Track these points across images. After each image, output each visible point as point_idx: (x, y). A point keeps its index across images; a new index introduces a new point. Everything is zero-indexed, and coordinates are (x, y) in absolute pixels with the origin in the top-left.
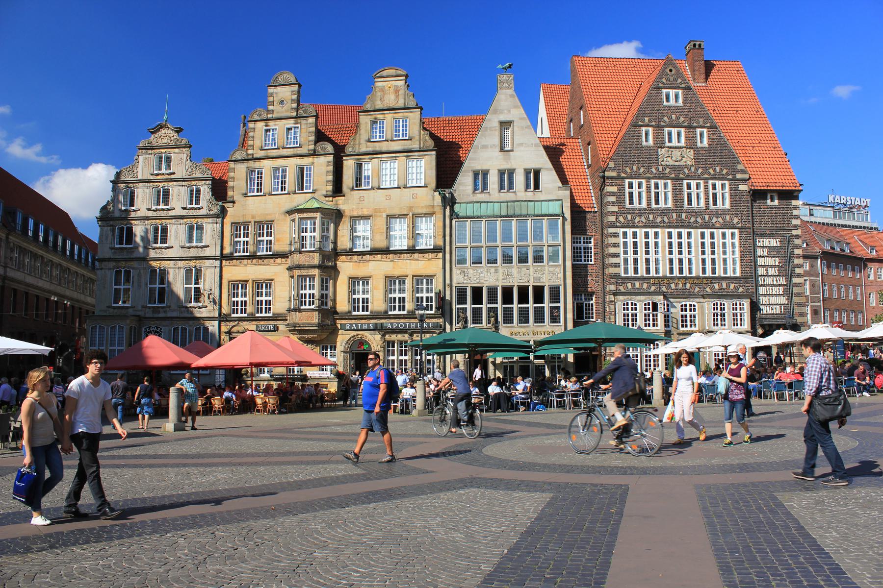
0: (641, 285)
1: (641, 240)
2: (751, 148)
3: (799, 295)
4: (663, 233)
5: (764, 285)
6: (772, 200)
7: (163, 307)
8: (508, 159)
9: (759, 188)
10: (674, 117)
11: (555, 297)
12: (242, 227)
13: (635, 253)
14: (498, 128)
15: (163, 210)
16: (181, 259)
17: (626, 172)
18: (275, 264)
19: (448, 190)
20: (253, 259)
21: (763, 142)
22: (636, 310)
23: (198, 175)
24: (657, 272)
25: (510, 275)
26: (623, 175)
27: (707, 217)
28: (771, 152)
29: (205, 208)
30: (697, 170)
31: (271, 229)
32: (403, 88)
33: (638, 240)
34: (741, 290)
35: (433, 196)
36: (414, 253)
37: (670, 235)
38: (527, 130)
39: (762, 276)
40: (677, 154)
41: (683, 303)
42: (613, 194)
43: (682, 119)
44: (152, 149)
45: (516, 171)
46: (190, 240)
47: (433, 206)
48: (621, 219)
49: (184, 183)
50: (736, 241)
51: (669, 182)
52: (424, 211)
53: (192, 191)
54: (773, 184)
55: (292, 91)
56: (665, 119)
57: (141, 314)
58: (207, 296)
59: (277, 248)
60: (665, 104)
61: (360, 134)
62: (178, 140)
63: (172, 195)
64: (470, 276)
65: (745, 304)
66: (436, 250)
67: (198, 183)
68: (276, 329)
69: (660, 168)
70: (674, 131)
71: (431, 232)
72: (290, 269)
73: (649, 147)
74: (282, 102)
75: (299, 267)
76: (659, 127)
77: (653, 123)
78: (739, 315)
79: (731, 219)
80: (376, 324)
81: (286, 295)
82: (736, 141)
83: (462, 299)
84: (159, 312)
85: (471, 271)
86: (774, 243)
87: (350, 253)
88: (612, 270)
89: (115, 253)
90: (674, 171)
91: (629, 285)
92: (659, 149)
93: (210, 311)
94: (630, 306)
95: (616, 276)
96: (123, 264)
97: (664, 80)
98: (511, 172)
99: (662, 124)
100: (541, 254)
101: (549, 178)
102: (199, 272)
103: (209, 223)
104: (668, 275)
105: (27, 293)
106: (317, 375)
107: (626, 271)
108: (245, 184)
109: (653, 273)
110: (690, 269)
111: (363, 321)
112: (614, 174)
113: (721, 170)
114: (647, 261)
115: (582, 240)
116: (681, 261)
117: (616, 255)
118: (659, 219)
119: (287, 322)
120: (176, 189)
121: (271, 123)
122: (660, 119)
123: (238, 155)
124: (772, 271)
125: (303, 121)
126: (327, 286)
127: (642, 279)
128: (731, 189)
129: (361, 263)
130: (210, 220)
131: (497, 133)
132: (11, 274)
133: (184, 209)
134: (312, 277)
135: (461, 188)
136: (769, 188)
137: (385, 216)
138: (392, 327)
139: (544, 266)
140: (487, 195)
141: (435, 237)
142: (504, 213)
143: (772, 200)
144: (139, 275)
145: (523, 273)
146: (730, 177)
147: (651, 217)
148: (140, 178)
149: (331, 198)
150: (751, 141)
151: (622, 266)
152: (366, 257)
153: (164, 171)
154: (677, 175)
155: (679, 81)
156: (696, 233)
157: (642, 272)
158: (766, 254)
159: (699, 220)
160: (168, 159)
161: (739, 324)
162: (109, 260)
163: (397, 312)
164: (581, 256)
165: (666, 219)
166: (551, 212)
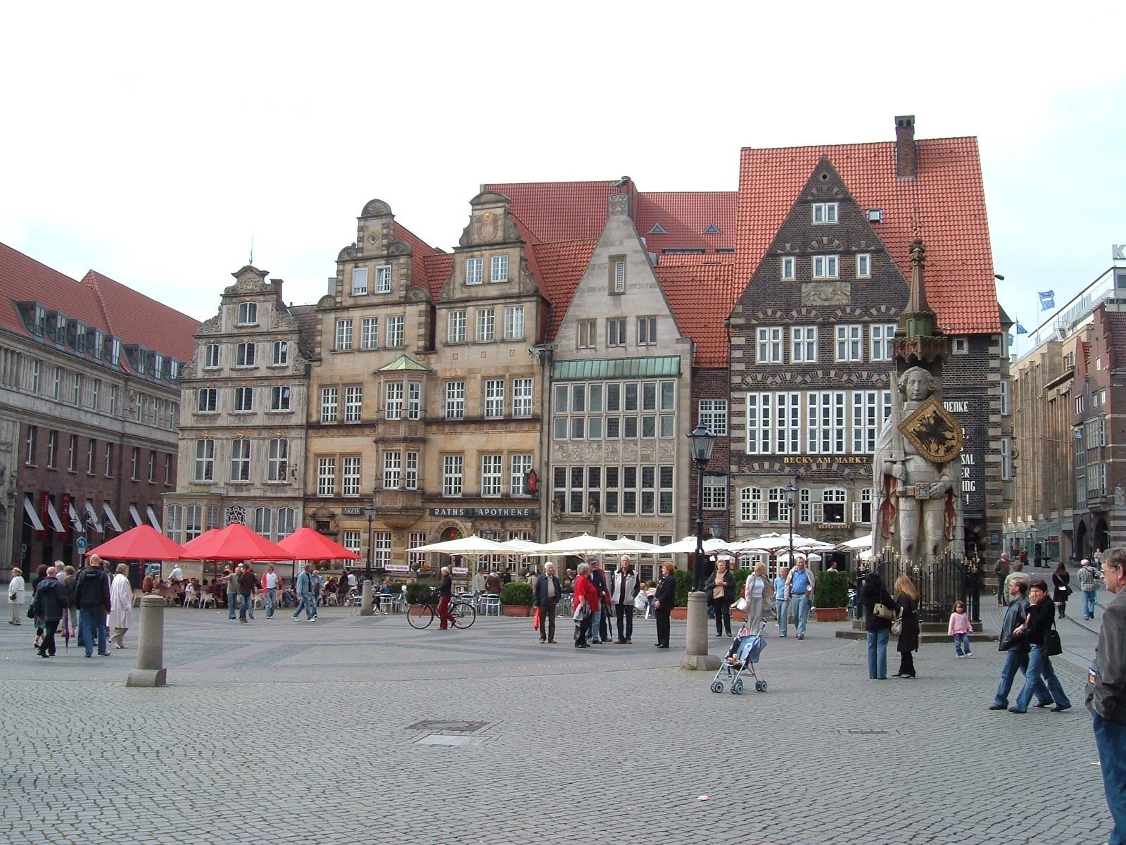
0: (772, 466)
1: (774, 406)
3: (994, 478)
4: (804, 397)
7: (247, 485)
8: (617, 305)
10: (825, 239)
11: (666, 480)
13: (766, 423)
15: (246, 369)
17: (757, 318)
18: (363, 436)
19: (549, 345)
23: (284, 328)
24: (795, 447)
25: (615, 452)
26: (754, 322)
27: (865, 374)
29: (291, 367)
30: (853, 311)
33: (770, 407)
41: (828, 489)
42: (738, 347)
43: (837, 242)
44: (236, 297)
45: (628, 319)
46: (275, 406)
49: (269, 338)
52: (522, 371)
55: (383, 224)
56: (814, 243)
57: (221, 491)
60: (814, 223)
63: (257, 352)
66: (536, 420)
67: (284, 337)
68: (362, 514)
69: (804, 311)
70: (825, 259)
72: (376, 442)
73: (790, 283)
76: (804, 257)
77: (797, 251)
80: (467, 510)
81: (372, 472)
83: (560, 480)
84: (242, 491)
87: (440, 422)
88: (734, 446)
91: (756, 466)
92: (804, 285)
95: (741, 456)
96: (205, 434)
97: (814, 191)
98: (623, 322)
99: (809, 250)
101: (667, 329)
102: (284, 443)
103: (295, 385)
104: (809, 452)
107: (753, 448)
112: (741, 321)
113: (888, 309)
115: (713, 405)
118: (799, 379)
120: (261, 345)
122: (806, 244)
125: (395, 262)
126: (414, 463)
127: (773, 458)
129: (453, 436)
130: (296, 382)
131: (607, 271)
132: (130, 429)
133: (268, 368)
135: (564, 342)
137: (479, 377)
138: (484, 512)
139: (655, 440)
140: (593, 351)
142: (610, 373)
147: (788, 376)
148: (223, 331)
149: (423, 356)
151: (748, 440)
152: (459, 428)
155: (836, 190)
156: (848, 396)
157: (774, 449)
159: (854, 378)
160: (253, 307)
162: (192, 429)
165: (808, 379)
166: (666, 371)
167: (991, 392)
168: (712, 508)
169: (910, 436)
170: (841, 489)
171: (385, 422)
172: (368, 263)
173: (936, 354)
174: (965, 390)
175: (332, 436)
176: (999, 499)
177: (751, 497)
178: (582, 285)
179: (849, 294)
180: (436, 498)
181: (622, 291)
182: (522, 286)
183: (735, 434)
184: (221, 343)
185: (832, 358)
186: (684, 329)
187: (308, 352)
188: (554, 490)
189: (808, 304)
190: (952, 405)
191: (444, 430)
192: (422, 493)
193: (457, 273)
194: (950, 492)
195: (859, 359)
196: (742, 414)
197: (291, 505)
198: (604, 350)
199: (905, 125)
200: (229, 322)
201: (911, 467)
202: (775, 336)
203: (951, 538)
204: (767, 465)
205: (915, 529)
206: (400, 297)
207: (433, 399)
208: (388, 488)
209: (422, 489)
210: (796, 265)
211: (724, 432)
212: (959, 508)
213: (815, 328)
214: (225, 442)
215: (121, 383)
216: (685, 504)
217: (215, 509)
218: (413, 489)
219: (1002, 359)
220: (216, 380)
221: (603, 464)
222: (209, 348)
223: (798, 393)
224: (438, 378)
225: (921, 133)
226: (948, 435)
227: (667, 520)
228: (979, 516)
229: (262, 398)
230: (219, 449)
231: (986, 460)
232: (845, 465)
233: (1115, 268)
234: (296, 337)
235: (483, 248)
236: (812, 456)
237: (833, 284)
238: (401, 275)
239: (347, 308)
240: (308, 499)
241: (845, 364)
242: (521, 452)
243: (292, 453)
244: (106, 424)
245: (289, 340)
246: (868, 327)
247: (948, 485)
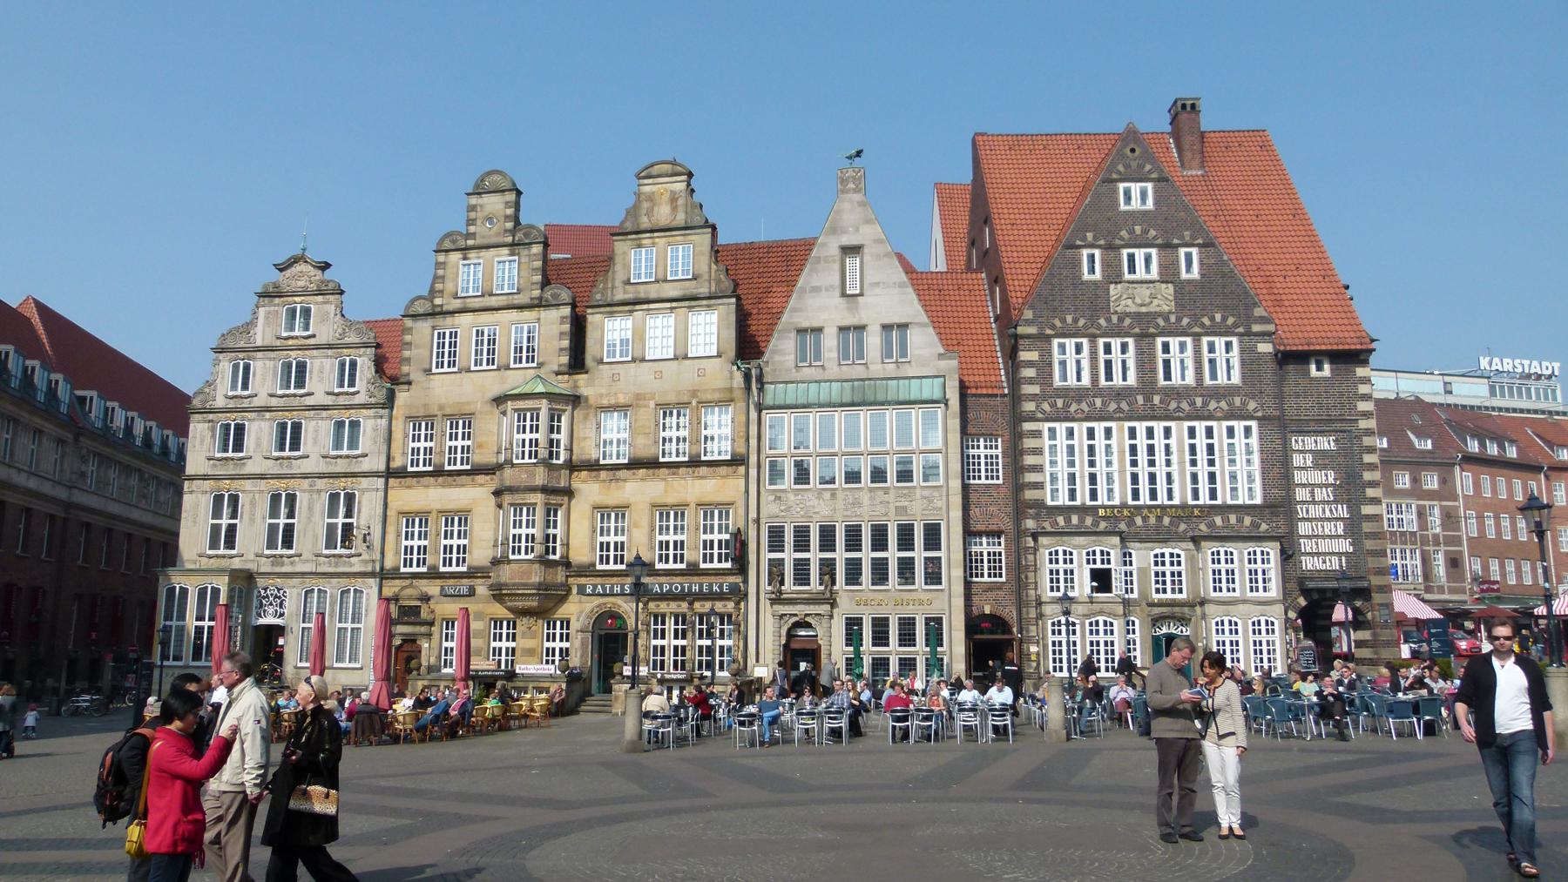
0: (1082, 520)
1: (1081, 441)
2: (1281, 279)
4: (1121, 429)
5: (1308, 520)
6: (1319, 369)
7: (290, 557)
8: (853, 309)
9: (1294, 348)
10: (1138, 229)
12: (423, 424)
14: (838, 258)
16: (321, 476)
17: (1053, 327)
18: (474, 485)
19: (754, 363)
20: (439, 476)
21: (1304, 267)
22: (1071, 561)
23: (352, 338)
25: (857, 503)
26: (1049, 332)
27: (1199, 401)
28: (1318, 285)
29: (363, 392)
30: (1179, 319)
31: (469, 428)
32: (683, 194)
33: (1075, 442)
34: (1264, 527)
35: (731, 372)
36: (699, 466)
37: (1133, 433)
38: (886, 259)
39: (1303, 502)
40: (1143, 293)
41: (1158, 551)
42: (1030, 364)
43: (1153, 233)
45: (868, 328)
46: (338, 444)
47: (731, 390)
48: (1046, 406)
49: (330, 352)
50: (1254, 440)
51: (1130, 341)
52: (716, 396)
53: (342, 365)
54: (1320, 340)
55: (507, 203)
56: (1123, 233)
57: (252, 567)
58: (360, 537)
59: (478, 458)
60: (1123, 207)
61: (614, 272)
62: (322, 282)
63: (311, 372)
64: (790, 504)
65: (1272, 553)
66: (738, 461)
69: (1115, 319)
70: (1139, 254)
71: (727, 431)
72: (497, 493)
73: (1095, 283)
74: (489, 219)
75: (511, 490)
76: (1111, 248)
77: (1102, 242)
78: (1260, 572)
79: (1244, 404)
81: (490, 535)
82: (1254, 268)
85: (791, 497)
86: (1326, 443)
87: (593, 466)
88: (1029, 495)
89: (214, 465)
90: (1139, 323)
91: (1061, 520)
92: (1112, 286)
93: (365, 562)
94: (1061, 557)
95: (1040, 504)
97: (1121, 168)
99: (1118, 242)
100: (907, 467)
101: (923, 342)
102: (350, 498)
103: (369, 417)
104: (1130, 502)
105: (110, 531)
106: (532, 671)
108: (428, 353)
109: (1102, 499)
110: (1170, 491)
111: (615, 580)
112: (1032, 330)
113: (1224, 319)
114: (1093, 478)
116: (1152, 478)
117: (1038, 469)
118: (1113, 406)
119: (490, 581)
120: (317, 362)
121: (472, 254)
122: (1116, 235)
123: (420, 308)
124: (1320, 494)
125: (524, 252)
126: (555, 522)
127: (1083, 510)
128: (1242, 351)
130: (371, 412)
131: (837, 266)
133: (328, 393)
134: (532, 507)
135: (777, 358)
136: (1312, 348)
137: (652, 404)
138: (661, 589)
139: (914, 487)
140: (820, 370)
141: (733, 440)
142: (847, 399)
143: (1319, 369)
144: (253, 503)
145: (878, 501)
146: (1241, 330)
147: (1098, 402)
148: (259, 343)
150: (1281, 267)
152: (622, 473)
153: (296, 333)
154: (1145, 329)
155: (1148, 167)
156: (1179, 428)
157: (1083, 497)
158: (1309, 463)
159: (1185, 405)
160: (306, 312)
161: (1261, 589)
162: (205, 478)
163: (671, 566)
164: (979, 471)
165: (1124, 406)
166: (926, 395)
168: (986, 579)
170: (1176, 551)
171: (513, 465)
172: (484, 253)
174: (1330, 421)
175: (427, 486)
177: (1061, 561)
178: (800, 284)
179: (1171, 298)
180: (588, 570)
181: (858, 292)
182: (713, 284)
183: (1031, 477)
184: (254, 359)
185: (1154, 381)
186: (951, 340)
187: (389, 375)
188: (767, 556)
189: (1118, 309)
190: (1316, 442)
191: (599, 476)
192: (566, 563)
193: (618, 267)
195: (1190, 379)
196: (1038, 452)
197: (359, 583)
198: (836, 368)
199: (1183, 112)
200: (268, 330)
202: (1079, 349)
204: (1075, 519)
206: (531, 299)
207: (582, 435)
208: (516, 557)
209: (567, 557)
210: (1103, 260)
211: (998, 478)
213: (1130, 341)
214: (257, 496)
215: (69, 437)
216: (958, 573)
217: (241, 591)
218: (557, 557)
220: (244, 410)
221: (840, 520)
222: (236, 367)
223: (1113, 424)
224: (589, 407)
225: (1207, 122)
227: (934, 594)
229: (317, 434)
230: (247, 507)
231: (1363, 513)
232: (1179, 517)
234: (371, 351)
235: (656, 234)
236: (1136, 507)
237: (1151, 285)
238: (533, 269)
239: (452, 313)
240: (384, 575)
241: (1173, 388)
242: (718, 505)
243: (363, 510)
244: (47, 488)
245: (360, 356)
246: (1199, 340)
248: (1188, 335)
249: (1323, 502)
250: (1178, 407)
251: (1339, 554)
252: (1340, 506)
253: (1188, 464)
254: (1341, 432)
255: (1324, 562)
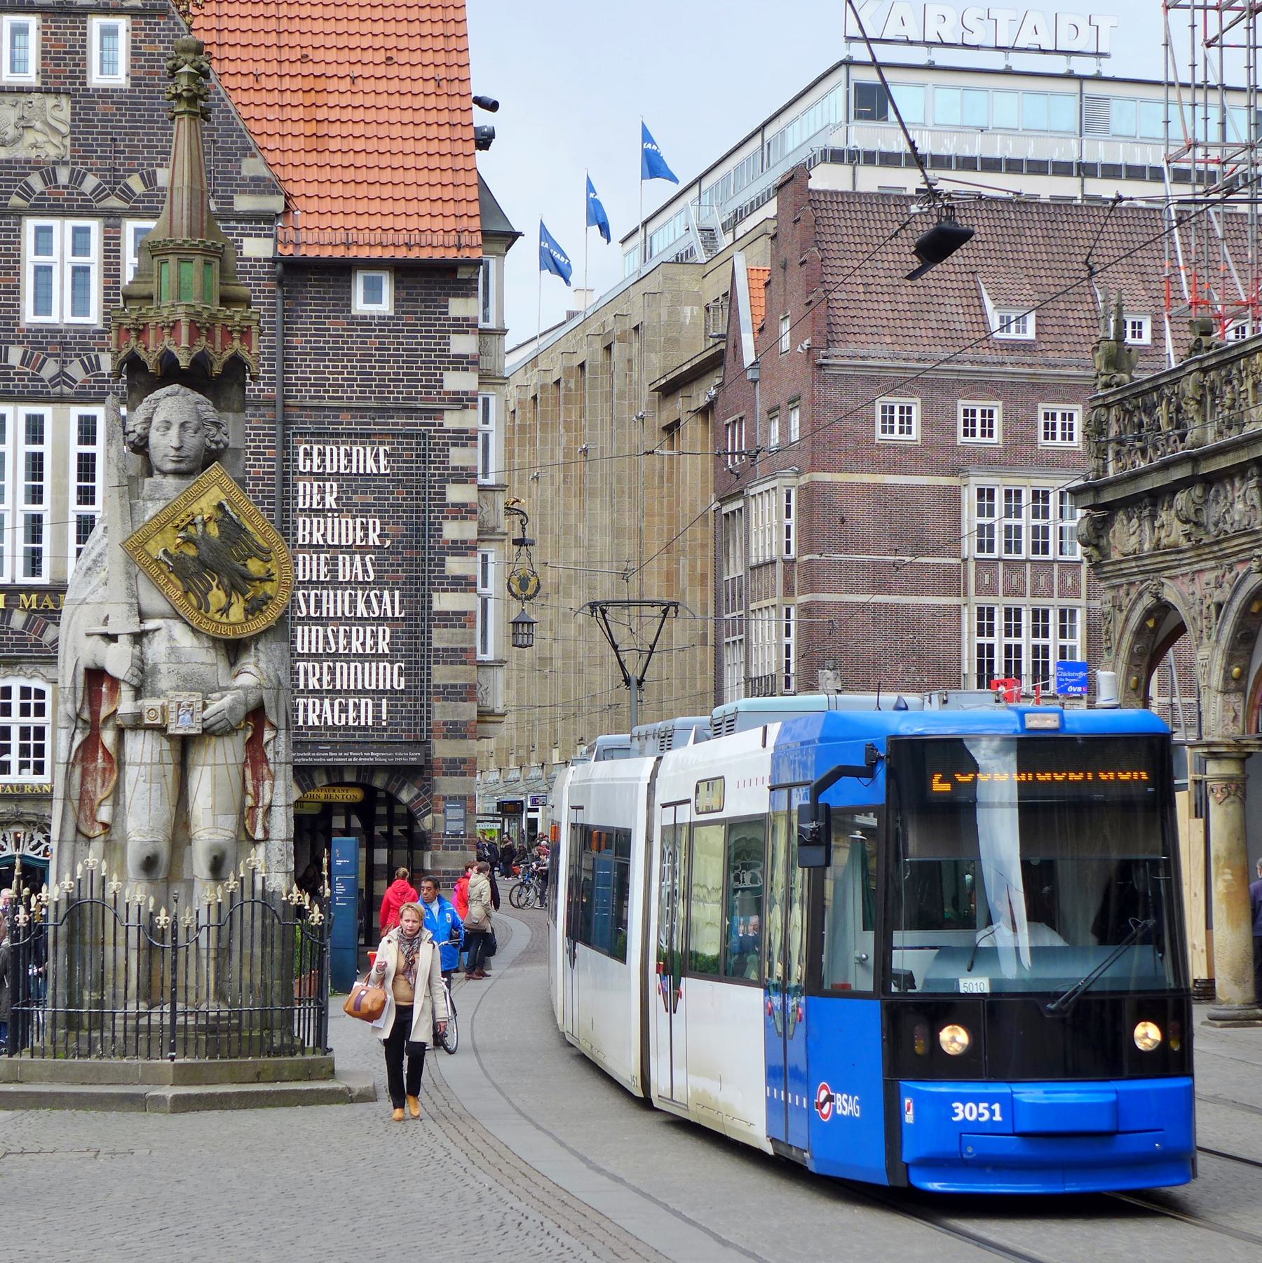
6: (373, 294)
30: (77, 178)
124: (349, 568)
136: (353, 253)
143: (373, 294)
158: (330, 501)
159: (76, 370)
167: (452, 420)
169: (154, 570)
170: (35, 684)
173: (228, 353)
176: (468, 711)
179: (65, 129)
190: (348, 455)
194: (257, 715)
201: (156, 650)
203: (259, 834)
205: (165, 812)
212: (282, 758)
219: (484, 333)
226: (255, 566)
228: (413, 757)
231: (436, 606)
233: (848, 63)
237: (23, 99)
241: (53, 331)
247: (252, 699)
248: (92, 215)
249: (354, 584)
250: (62, 373)
251: (377, 693)
252: (386, 593)
253: (73, 495)
254: (405, 436)
255: (344, 709)
